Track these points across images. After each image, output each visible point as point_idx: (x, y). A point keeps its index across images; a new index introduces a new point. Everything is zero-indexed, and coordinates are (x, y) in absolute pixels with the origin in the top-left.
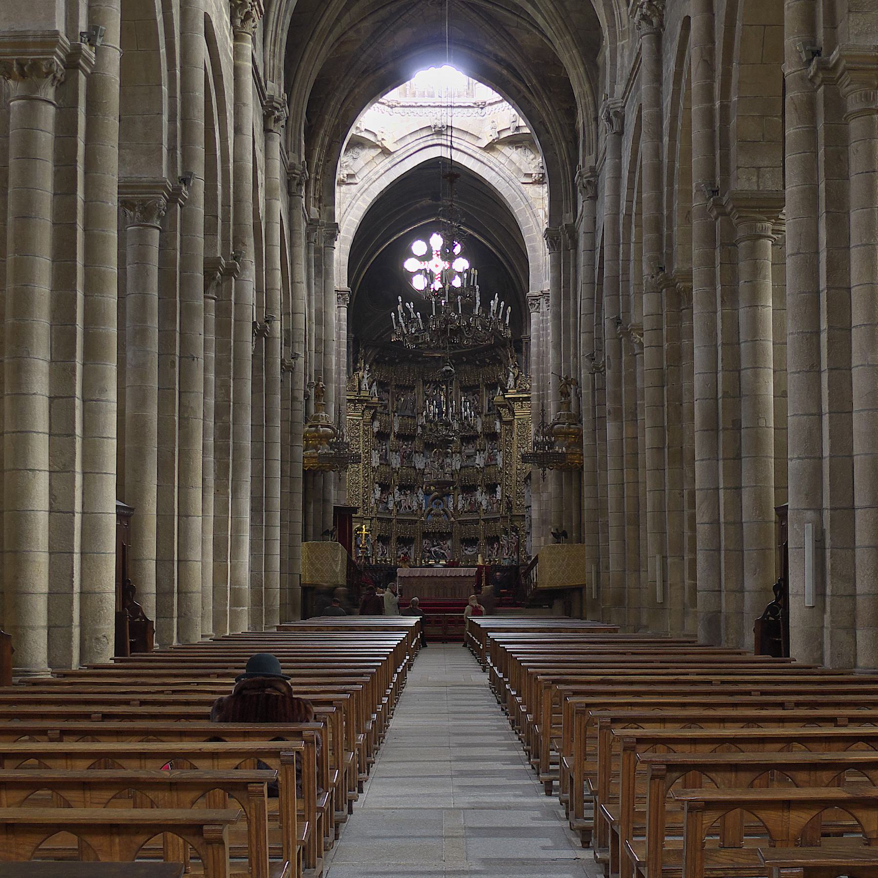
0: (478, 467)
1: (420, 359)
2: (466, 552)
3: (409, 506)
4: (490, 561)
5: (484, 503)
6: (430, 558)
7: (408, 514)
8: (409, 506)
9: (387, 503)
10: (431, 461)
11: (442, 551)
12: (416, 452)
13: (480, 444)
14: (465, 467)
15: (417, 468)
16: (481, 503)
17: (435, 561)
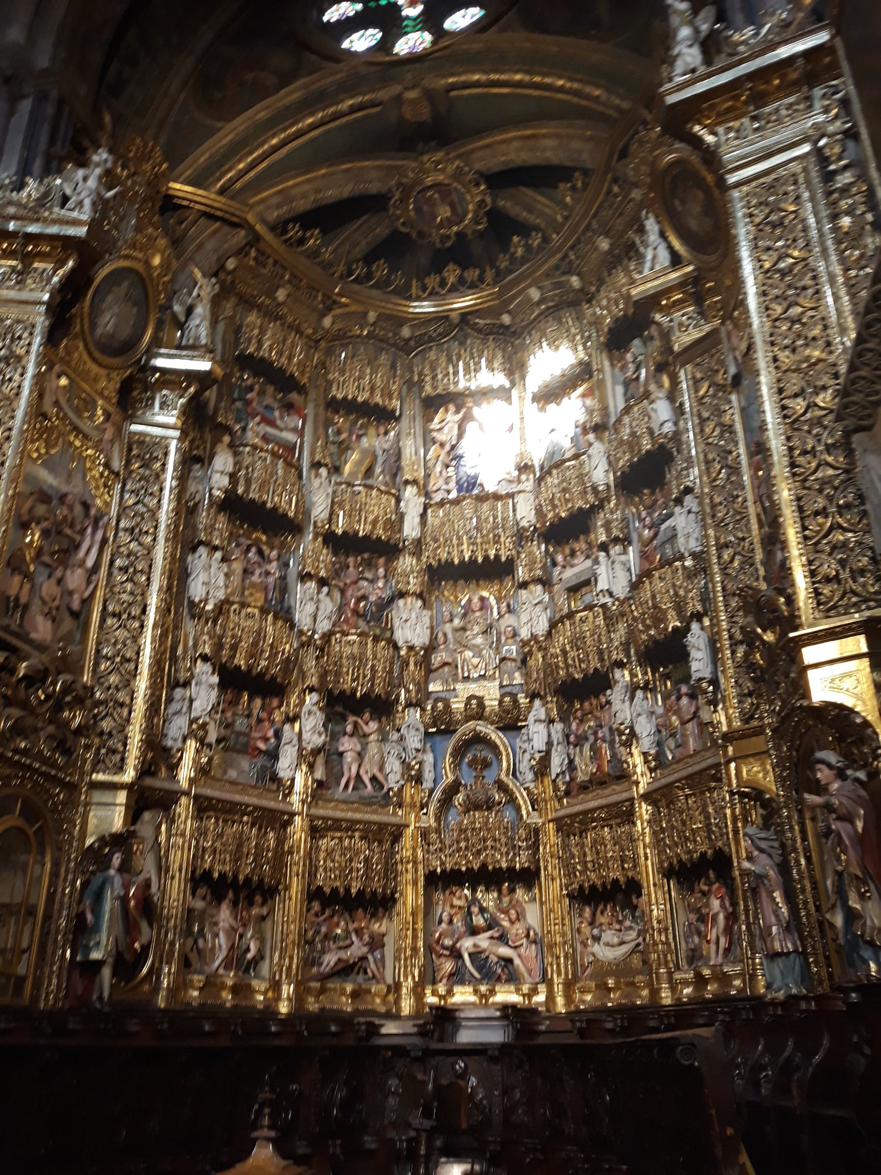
0: (607, 600)
1: (406, 332)
2: (597, 948)
3: (374, 779)
4: (700, 981)
5: (645, 728)
6: (458, 977)
7: (367, 802)
8: (374, 779)
9: (273, 755)
10: (456, 630)
11: (504, 951)
12: (402, 595)
13: (607, 526)
14: (561, 620)
15: (400, 643)
16: (632, 728)
17: (476, 991)
